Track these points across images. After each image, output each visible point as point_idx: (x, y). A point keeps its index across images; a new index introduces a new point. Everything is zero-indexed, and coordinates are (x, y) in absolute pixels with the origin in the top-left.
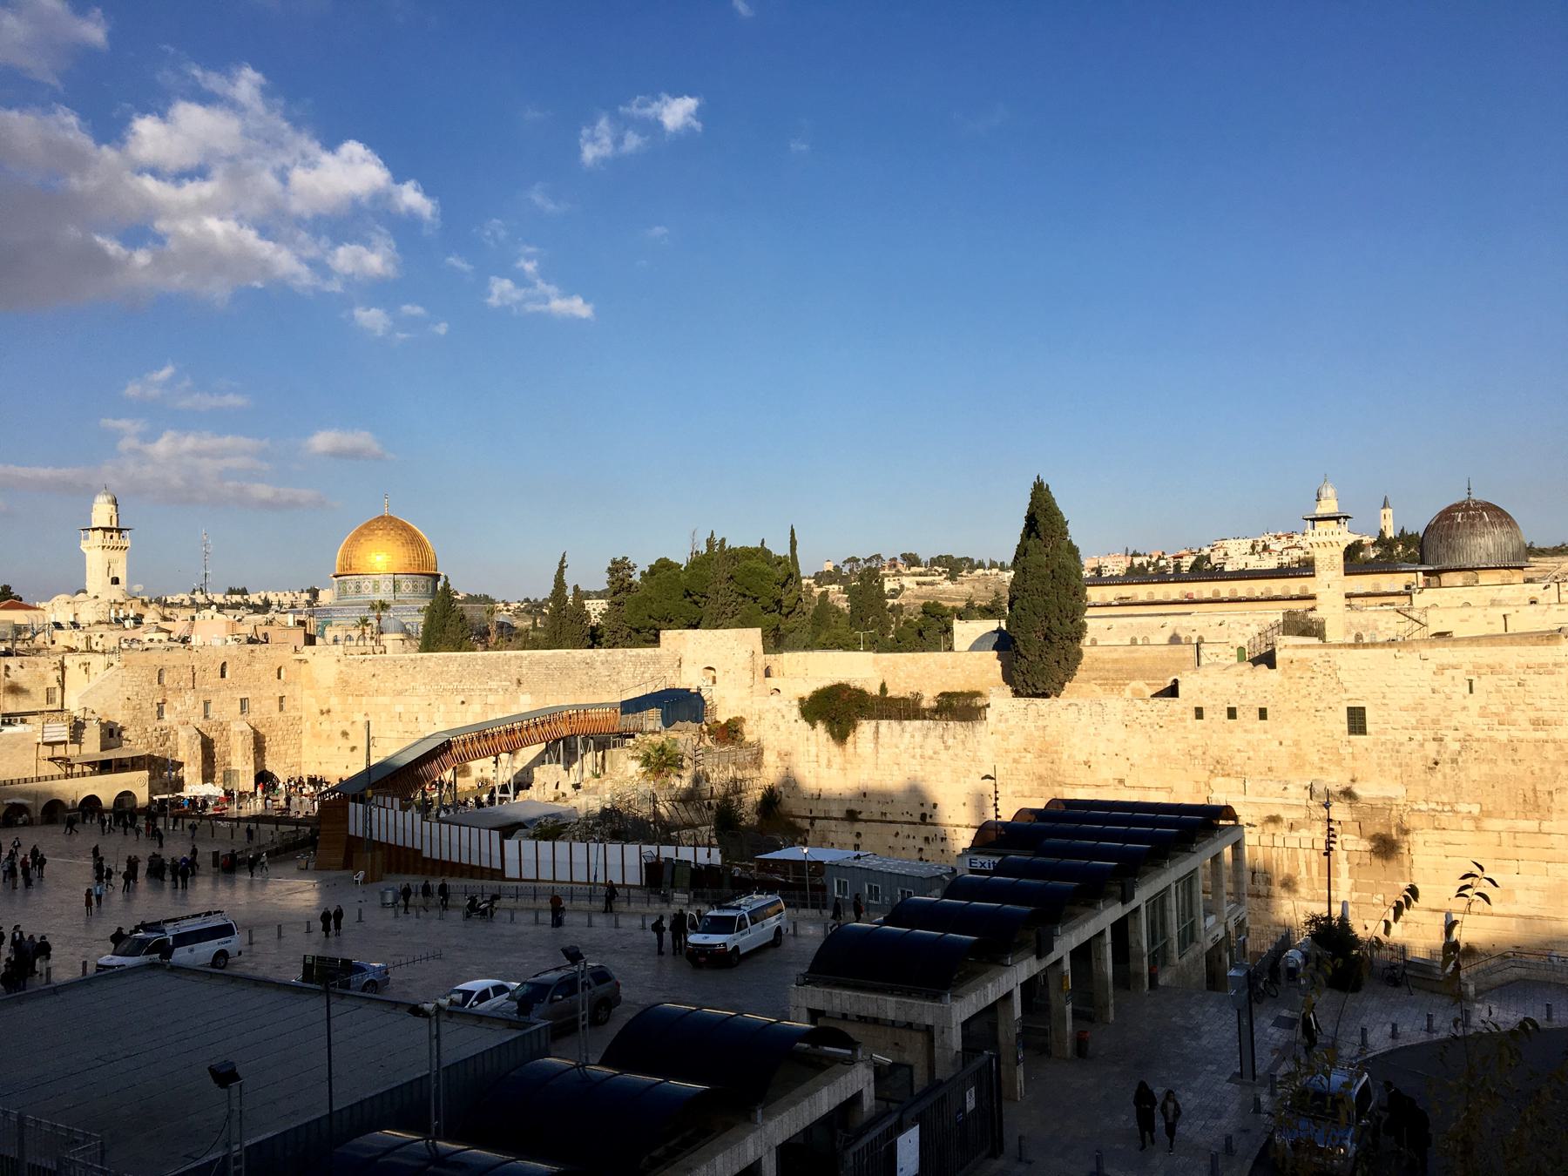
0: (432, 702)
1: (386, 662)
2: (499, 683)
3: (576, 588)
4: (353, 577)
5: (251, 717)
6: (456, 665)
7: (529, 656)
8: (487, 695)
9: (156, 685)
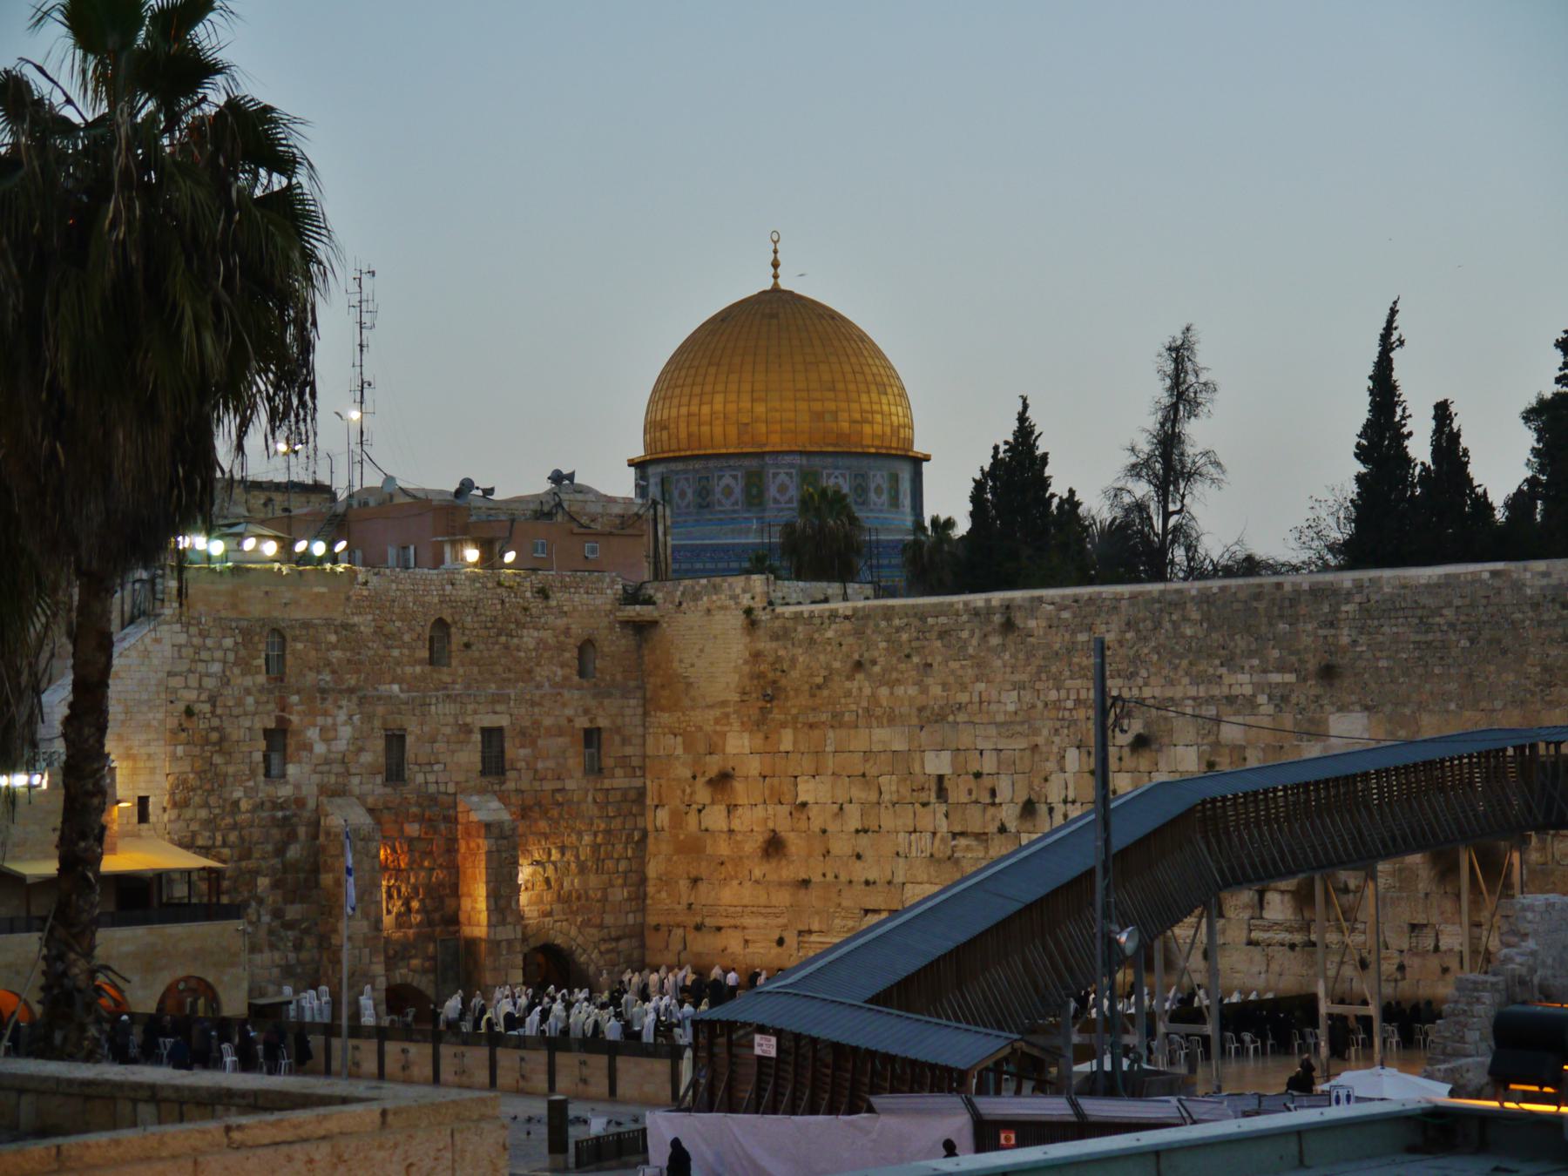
0: (1040, 740)
1: (897, 622)
2: (1256, 678)
3: (1442, 412)
4: (691, 465)
5: (510, 785)
6: (1116, 623)
7: (1359, 586)
8: (1218, 721)
9: (261, 679)
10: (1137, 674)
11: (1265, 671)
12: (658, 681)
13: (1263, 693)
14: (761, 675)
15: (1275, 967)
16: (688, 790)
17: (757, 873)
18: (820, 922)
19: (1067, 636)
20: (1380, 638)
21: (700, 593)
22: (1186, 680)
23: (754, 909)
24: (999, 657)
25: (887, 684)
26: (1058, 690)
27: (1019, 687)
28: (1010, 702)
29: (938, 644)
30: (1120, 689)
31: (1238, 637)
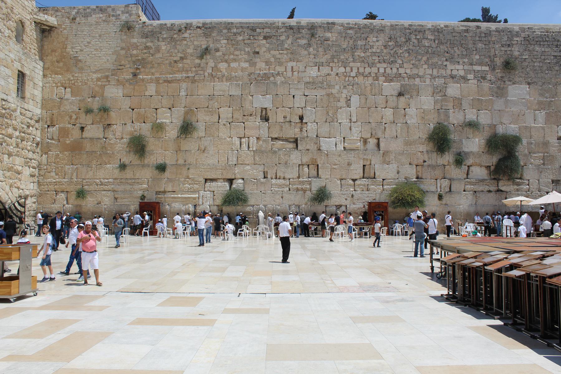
0: (334, 91)
1: (235, 30)
2: (466, 67)
10: (396, 62)
11: (471, 64)
12: (55, 59)
13: (470, 74)
14: (131, 56)
15: (480, 202)
16: (74, 117)
17: (126, 160)
18: (173, 186)
19: (351, 42)
20: (536, 53)
21: (90, 13)
22: (425, 66)
23: (121, 181)
24: (306, 50)
25: (226, 61)
26: (345, 68)
27: (319, 65)
28: (313, 72)
29: (264, 42)
30: (385, 68)
31: (456, 49)
